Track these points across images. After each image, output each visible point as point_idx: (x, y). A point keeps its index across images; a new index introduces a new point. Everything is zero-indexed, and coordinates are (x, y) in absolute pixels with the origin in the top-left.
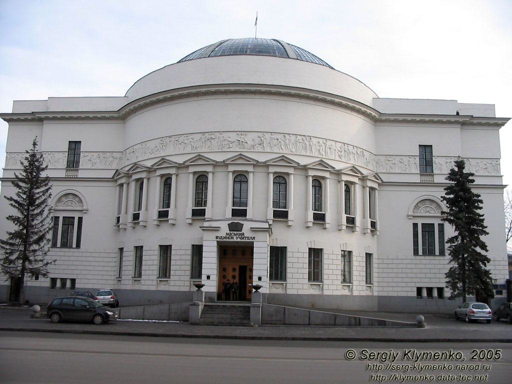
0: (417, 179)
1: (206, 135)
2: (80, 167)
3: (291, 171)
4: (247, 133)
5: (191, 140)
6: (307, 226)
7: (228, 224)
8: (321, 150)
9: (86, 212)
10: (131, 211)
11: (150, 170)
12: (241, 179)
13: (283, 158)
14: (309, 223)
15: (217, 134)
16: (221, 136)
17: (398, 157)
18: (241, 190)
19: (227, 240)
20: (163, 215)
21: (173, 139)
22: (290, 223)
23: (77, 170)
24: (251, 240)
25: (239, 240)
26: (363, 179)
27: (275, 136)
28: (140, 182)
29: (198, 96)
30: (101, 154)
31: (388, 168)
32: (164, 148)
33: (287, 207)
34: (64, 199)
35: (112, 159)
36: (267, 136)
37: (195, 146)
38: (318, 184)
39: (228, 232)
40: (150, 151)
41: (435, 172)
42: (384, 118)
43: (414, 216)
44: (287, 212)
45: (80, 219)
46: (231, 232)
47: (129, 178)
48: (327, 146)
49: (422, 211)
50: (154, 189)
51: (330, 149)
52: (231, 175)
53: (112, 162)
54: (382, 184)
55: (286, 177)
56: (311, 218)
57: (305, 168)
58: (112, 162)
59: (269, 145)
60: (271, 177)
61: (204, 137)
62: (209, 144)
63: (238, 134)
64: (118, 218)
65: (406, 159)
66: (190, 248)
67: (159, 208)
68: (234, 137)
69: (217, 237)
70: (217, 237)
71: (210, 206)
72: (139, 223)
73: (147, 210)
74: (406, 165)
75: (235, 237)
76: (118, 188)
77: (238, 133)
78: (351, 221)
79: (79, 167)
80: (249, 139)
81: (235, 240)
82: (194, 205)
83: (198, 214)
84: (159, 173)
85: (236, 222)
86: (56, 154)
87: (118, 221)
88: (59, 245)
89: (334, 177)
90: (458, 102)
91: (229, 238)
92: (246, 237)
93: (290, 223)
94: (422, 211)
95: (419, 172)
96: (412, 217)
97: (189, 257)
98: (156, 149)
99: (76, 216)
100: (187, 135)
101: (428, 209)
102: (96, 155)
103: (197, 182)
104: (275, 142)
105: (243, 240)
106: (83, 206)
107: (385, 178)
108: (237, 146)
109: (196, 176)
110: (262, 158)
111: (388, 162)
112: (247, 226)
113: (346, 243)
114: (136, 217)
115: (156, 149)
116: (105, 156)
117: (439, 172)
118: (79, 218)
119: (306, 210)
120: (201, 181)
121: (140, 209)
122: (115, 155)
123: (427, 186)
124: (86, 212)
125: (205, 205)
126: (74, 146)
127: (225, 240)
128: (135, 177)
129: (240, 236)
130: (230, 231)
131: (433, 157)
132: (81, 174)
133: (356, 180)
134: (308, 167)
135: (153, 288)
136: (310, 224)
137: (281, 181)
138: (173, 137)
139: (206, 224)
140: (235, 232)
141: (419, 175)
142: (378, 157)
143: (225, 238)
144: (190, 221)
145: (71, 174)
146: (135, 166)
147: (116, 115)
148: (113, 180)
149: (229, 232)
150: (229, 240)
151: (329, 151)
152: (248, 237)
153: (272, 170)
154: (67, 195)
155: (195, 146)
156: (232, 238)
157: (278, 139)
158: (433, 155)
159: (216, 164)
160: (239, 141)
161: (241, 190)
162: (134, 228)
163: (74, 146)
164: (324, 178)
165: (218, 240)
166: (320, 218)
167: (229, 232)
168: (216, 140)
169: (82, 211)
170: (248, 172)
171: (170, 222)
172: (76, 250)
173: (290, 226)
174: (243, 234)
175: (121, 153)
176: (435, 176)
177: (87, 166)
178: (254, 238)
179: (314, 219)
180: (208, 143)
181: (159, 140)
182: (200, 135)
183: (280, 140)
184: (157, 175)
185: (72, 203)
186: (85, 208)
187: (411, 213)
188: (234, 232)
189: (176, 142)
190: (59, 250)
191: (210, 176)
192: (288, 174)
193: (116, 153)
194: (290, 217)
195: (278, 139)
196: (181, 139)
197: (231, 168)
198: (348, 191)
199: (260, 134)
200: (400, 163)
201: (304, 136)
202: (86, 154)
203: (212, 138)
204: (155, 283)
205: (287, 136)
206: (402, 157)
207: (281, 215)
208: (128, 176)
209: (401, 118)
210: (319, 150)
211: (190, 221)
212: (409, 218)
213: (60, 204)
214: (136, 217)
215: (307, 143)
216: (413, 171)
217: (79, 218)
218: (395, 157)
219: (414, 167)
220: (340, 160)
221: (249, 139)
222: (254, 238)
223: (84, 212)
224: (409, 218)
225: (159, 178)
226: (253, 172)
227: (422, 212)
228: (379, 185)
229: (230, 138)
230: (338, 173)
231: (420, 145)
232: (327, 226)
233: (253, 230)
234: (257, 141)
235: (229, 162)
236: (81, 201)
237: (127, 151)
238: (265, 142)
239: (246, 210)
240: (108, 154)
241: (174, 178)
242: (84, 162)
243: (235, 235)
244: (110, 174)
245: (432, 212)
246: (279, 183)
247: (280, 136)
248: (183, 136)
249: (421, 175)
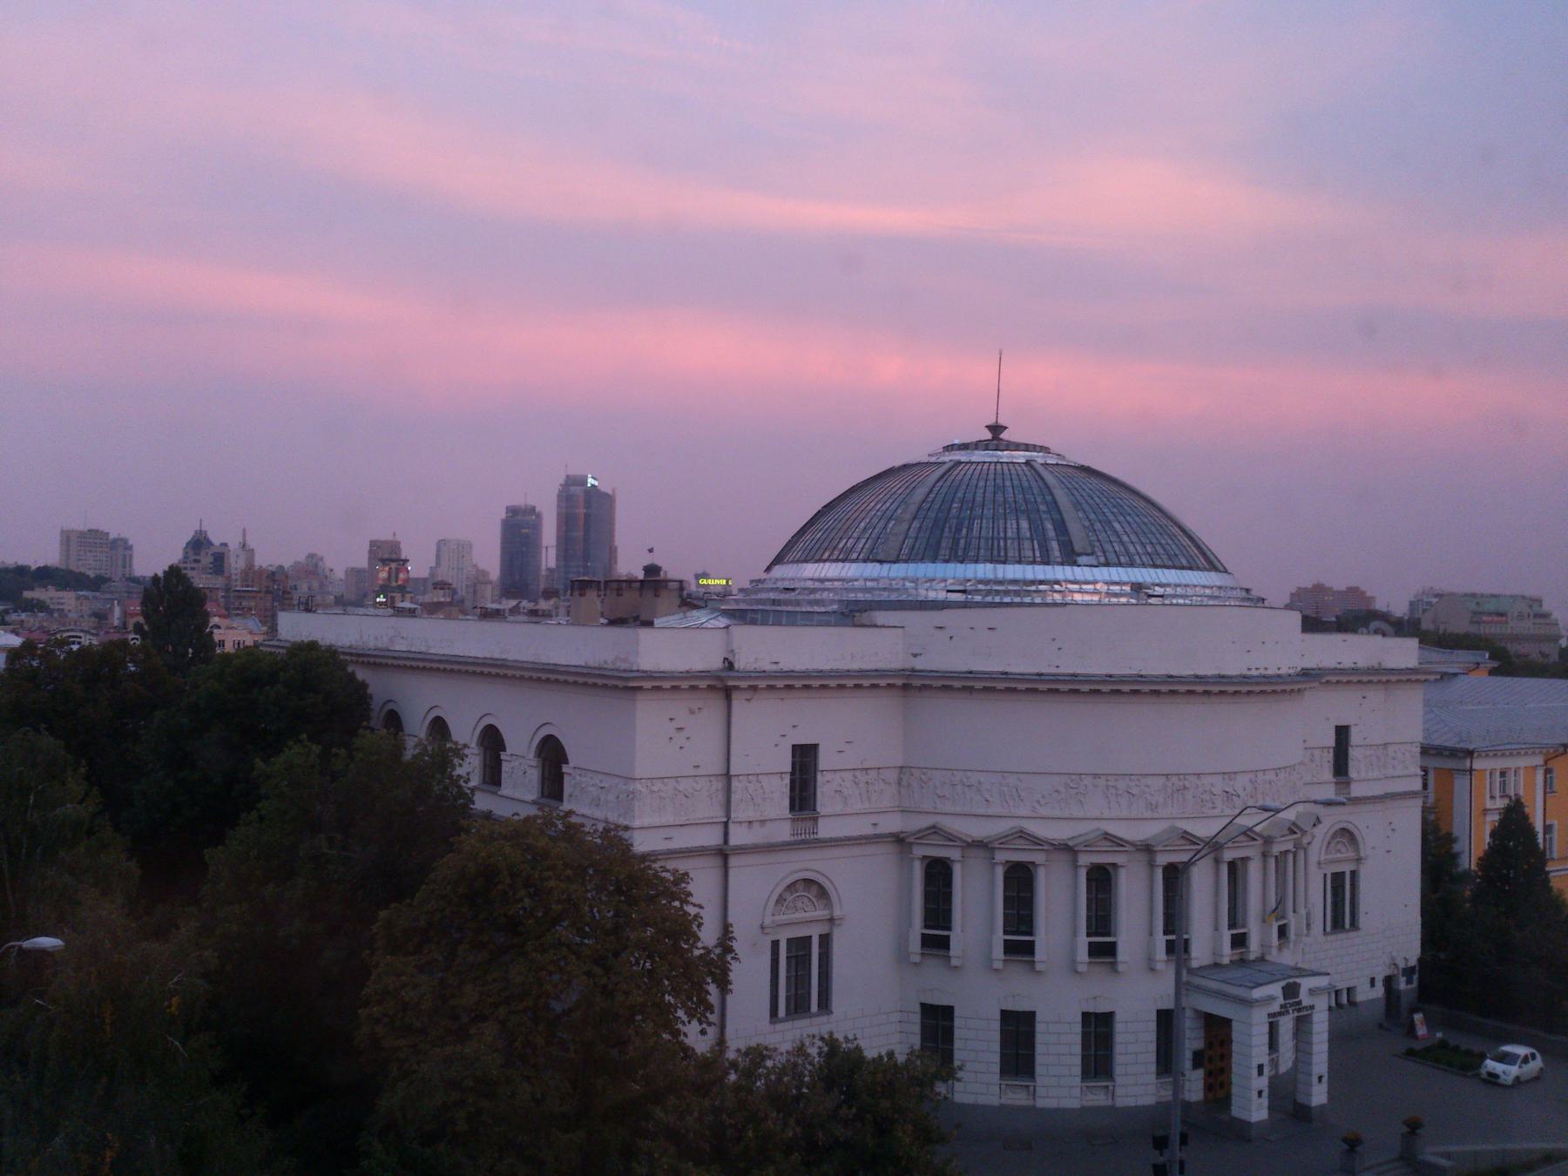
21: (1102, 782)
30: (858, 773)
66: (1154, 1017)
80: (1240, 783)
88: (782, 1012)
97: (1154, 1037)
99: (815, 932)
102: (848, 776)
126: (805, 759)
132: (825, 830)
135: (1074, 1104)
163: (805, 759)
172: (824, 1019)
190: (788, 1025)
196: (1121, 784)
199: (1251, 776)
202: (828, 776)
203: (1185, 788)
204: (1077, 1092)
221: (1240, 783)
222: (1312, 1007)
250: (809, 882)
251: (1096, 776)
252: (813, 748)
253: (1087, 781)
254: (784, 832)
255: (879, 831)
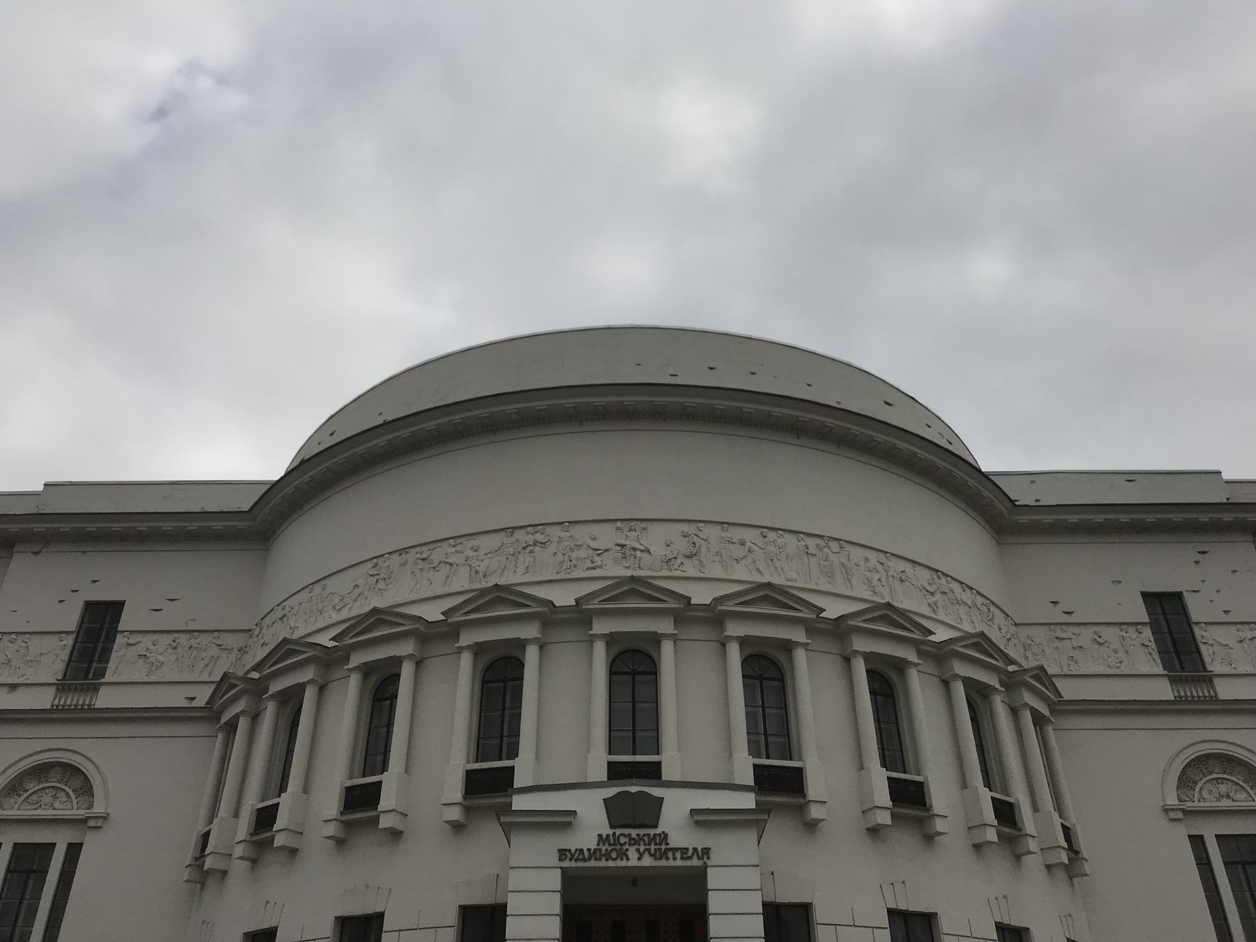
0: (1163, 691)
1: (520, 535)
2: (108, 677)
3: (798, 635)
4: (644, 525)
5: (471, 553)
6: (871, 825)
7: (604, 800)
8: (875, 581)
9: (99, 823)
10: (252, 801)
11: (331, 660)
12: (634, 669)
13: (769, 594)
14: (879, 813)
15: (556, 532)
16: (568, 534)
17: (1083, 630)
18: (634, 703)
19: (603, 863)
20: (360, 799)
21: (412, 556)
22: (815, 812)
23: (95, 689)
24: (695, 862)
25: (647, 861)
26: (1012, 683)
27: (736, 534)
28: (291, 701)
29: (494, 432)
30: (183, 639)
31: (1065, 662)
32: (381, 585)
33: (795, 755)
34: (32, 786)
35: (214, 651)
36: (711, 532)
37: (481, 570)
38: (886, 688)
39: (606, 830)
40: (337, 600)
41: (1215, 667)
42: (1024, 519)
43: (1185, 812)
44: (800, 771)
45: (74, 850)
46: (618, 832)
47: (258, 697)
48: (890, 573)
49: (1205, 794)
50: (338, 720)
51: (902, 581)
52: (600, 649)
53: (215, 659)
54: (1062, 707)
55: (782, 658)
56: (882, 795)
57: (839, 630)
58: (215, 659)
59: (717, 559)
60: (734, 654)
61: (513, 540)
62: (529, 560)
63: (618, 528)
64: (206, 836)
65: (1110, 634)
66: (452, 917)
67: (351, 778)
68: (606, 536)
69: (563, 854)
70: (563, 854)
71: (532, 756)
72: (272, 839)
73: (306, 790)
74: (1115, 652)
75: (633, 854)
76: (220, 736)
77: (619, 524)
78: (1006, 813)
79: (103, 675)
80: (657, 540)
81: (633, 861)
82: (473, 757)
83: (488, 786)
84: (357, 659)
85: (634, 789)
86: (36, 640)
87: (204, 845)
89: (930, 667)
90: (1226, 476)
91: (608, 856)
92: (675, 850)
93: (815, 812)
94: (1205, 794)
95: (1160, 670)
96: (1180, 815)
98: (356, 592)
100: (458, 541)
101: (1223, 788)
102: (165, 640)
103: (484, 682)
104: (738, 552)
105: (663, 863)
106: (90, 806)
107: (1068, 690)
108: (616, 562)
109: (485, 660)
110: (701, 595)
111: (1057, 643)
112: (676, 810)
113: (1005, 897)
114: (266, 818)
115: (356, 592)
116: (193, 642)
117: (1227, 670)
118: (70, 845)
119: (862, 768)
120: (500, 679)
121: (282, 788)
122: (227, 640)
123: (1201, 712)
124: (99, 823)
125: (513, 753)
127: (593, 863)
128: (277, 686)
129: (653, 847)
130: (612, 827)
131: (1195, 628)
132: (106, 699)
133: (991, 680)
134: (851, 623)
136: (884, 818)
137: (767, 673)
138: (413, 551)
139: (519, 803)
140: (634, 833)
141: (1165, 683)
142: (1023, 633)
143: (594, 854)
144: (455, 814)
145: (71, 700)
146: (286, 648)
147: (242, 524)
148: (210, 713)
149: (610, 832)
150: (611, 864)
151: (897, 585)
152: (684, 851)
153: (735, 629)
154: (41, 771)
155: (481, 570)
156: (623, 855)
157: (743, 543)
158: (1194, 618)
159: (550, 617)
160: (622, 546)
161: (634, 703)
162: (254, 862)
164: (901, 666)
165: (567, 864)
166: (909, 796)
167: (610, 832)
168: (552, 548)
169: (84, 821)
170: (656, 639)
171: (385, 822)
173: (811, 826)
174: (664, 837)
175: (246, 634)
176: (1216, 681)
177: (129, 677)
178: (706, 851)
179: (893, 798)
180: (524, 559)
181: (370, 565)
182: (501, 537)
183: (749, 544)
184: (350, 666)
185: (54, 797)
186: (98, 808)
187: (1172, 800)
188: (626, 831)
189: (421, 565)
191: (531, 657)
192: (788, 647)
193: (226, 635)
194: (814, 789)
195: (743, 543)
196: (438, 554)
197: (601, 627)
198: (975, 719)
199: (686, 528)
200: (1096, 646)
201: (821, 537)
203: (535, 543)
205: (772, 536)
206: (1098, 629)
207: (781, 784)
208: (257, 689)
209: (1073, 518)
210: (870, 581)
211: (455, 814)
212: (1172, 815)
213: (12, 801)
214: (266, 818)
215: (833, 558)
216: (1145, 670)
217: (70, 845)
218: (1076, 630)
219: (1144, 658)
220: (933, 615)
222: (706, 851)
223: (92, 823)
224: (1172, 815)
225: (354, 681)
226: (675, 638)
227: (1206, 796)
228: (1050, 705)
229: (595, 539)
230: (939, 655)
231: (1145, 595)
232: (940, 825)
233: (702, 819)
234: (681, 545)
235: (594, 605)
236: (86, 789)
237: (267, 620)
238: (703, 550)
239: (659, 764)
240: (205, 639)
241: (407, 671)
242: (123, 662)
243: (634, 842)
244: (202, 696)
245: (1242, 796)
246: (761, 678)
247: (751, 535)
248: (445, 544)
249: (1174, 680)
250: (71, 771)
251: (405, 550)
252: (115, 609)
253: (396, 559)
254: (43, 700)
255: (194, 704)
